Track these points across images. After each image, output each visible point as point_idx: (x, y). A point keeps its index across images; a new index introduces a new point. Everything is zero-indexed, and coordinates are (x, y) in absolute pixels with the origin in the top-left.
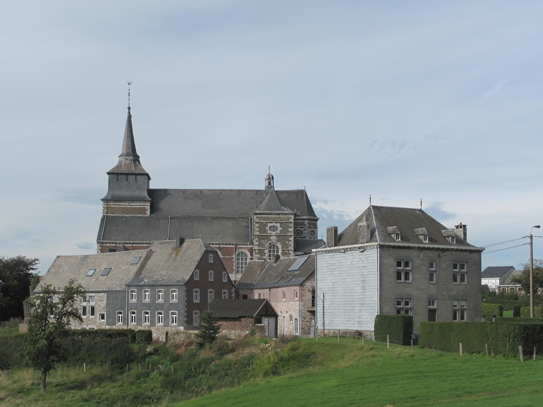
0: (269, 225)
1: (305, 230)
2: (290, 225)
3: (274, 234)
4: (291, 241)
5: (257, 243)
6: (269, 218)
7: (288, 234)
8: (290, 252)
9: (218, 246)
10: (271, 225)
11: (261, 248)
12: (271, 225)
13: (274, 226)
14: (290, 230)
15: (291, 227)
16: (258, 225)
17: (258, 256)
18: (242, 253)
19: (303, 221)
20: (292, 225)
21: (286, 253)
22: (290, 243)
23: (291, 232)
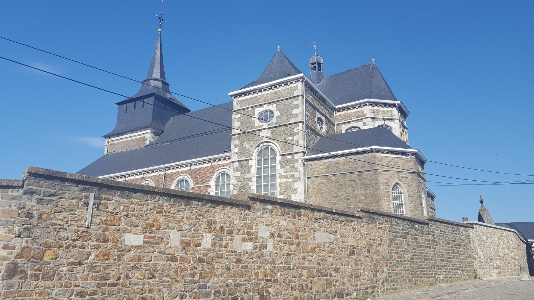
0: (258, 111)
1: (365, 124)
2: (295, 103)
3: (265, 125)
4: (297, 133)
5: (237, 150)
6: (257, 99)
7: (292, 121)
8: (296, 156)
9: (188, 168)
10: (261, 109)
11: (243, 158)
12: (261, 109)
13: (266, 111)
14: (295, 111)
15: (296, 106)
16: (239, 116)
17: (238, 174)
18: (223, 174)
19: (360, 109)
20: (300, 102)
21: (288, 161)
22: (296, 138)
23: (297, 116)
